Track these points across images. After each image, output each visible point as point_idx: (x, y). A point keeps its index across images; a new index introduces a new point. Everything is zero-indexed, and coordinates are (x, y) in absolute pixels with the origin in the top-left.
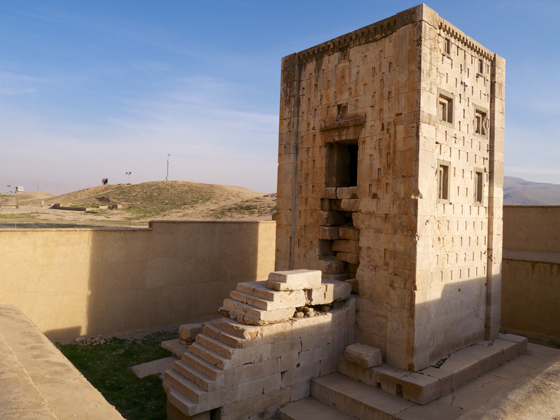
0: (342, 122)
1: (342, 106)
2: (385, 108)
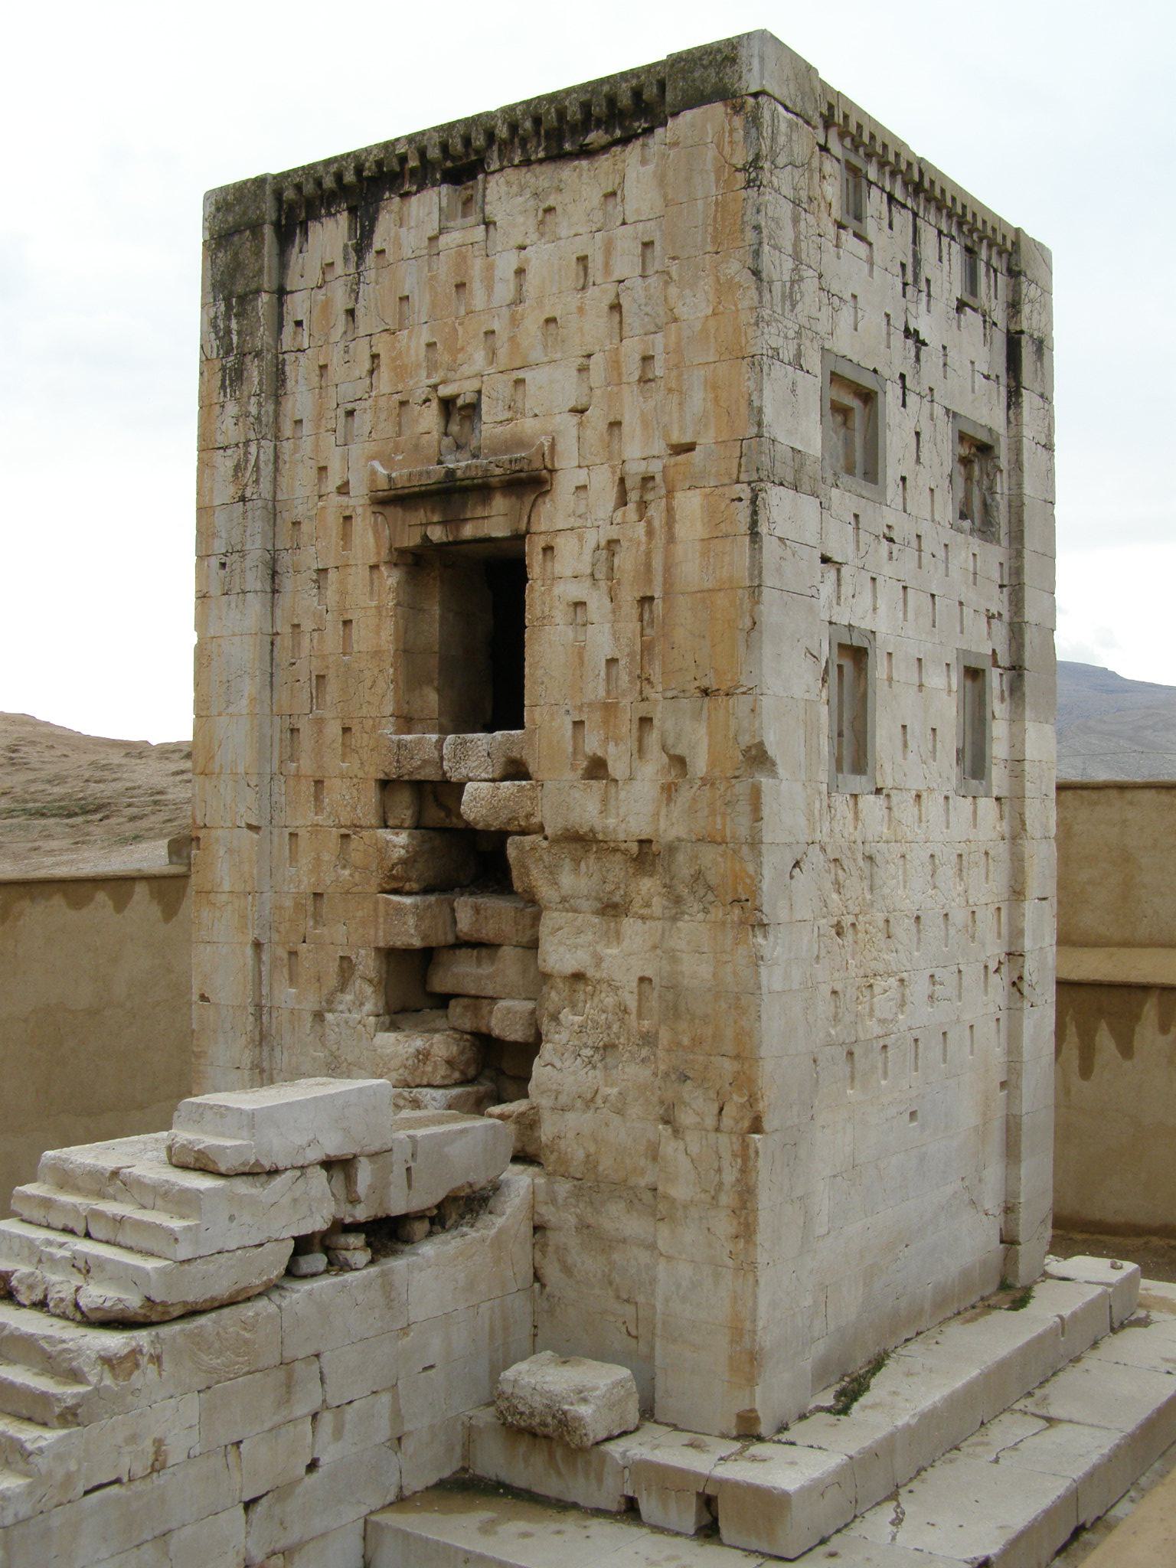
0: (459, 463)
1: (460, 402)
2: (631, 421)
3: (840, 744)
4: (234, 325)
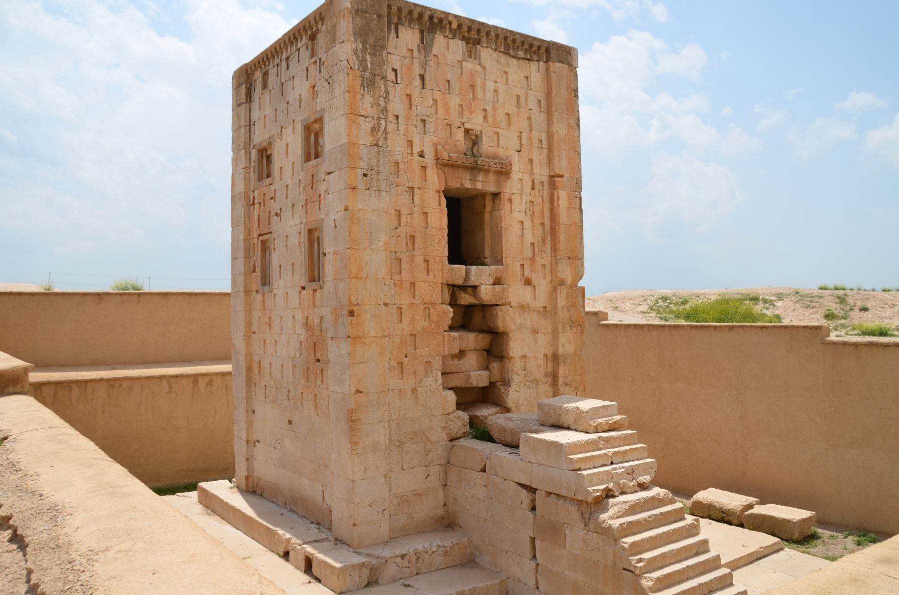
3: (319, 274)
4: (368, 57)
